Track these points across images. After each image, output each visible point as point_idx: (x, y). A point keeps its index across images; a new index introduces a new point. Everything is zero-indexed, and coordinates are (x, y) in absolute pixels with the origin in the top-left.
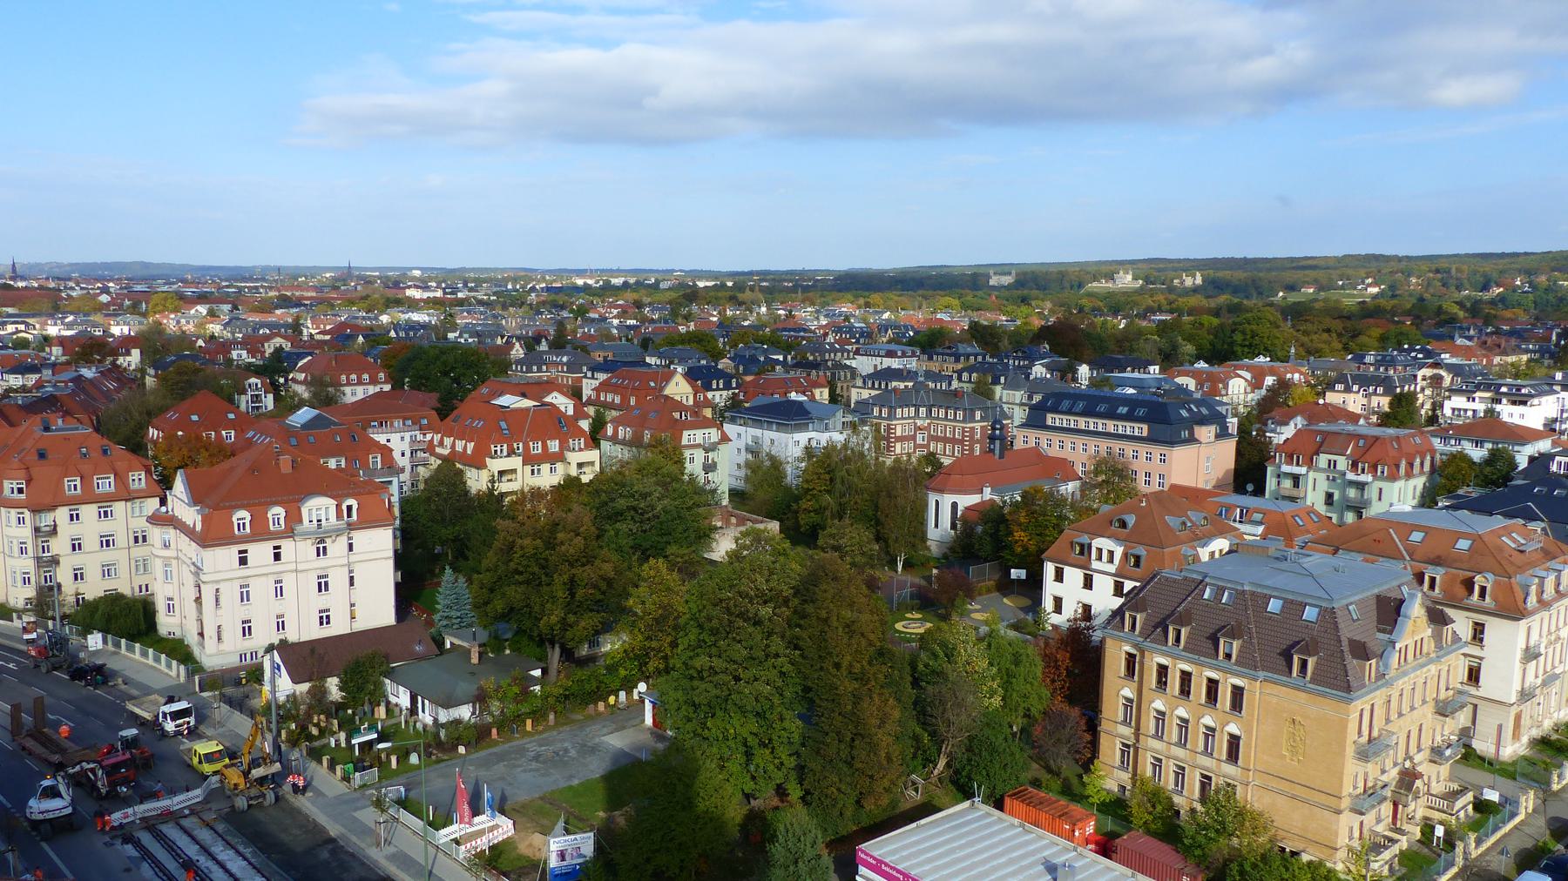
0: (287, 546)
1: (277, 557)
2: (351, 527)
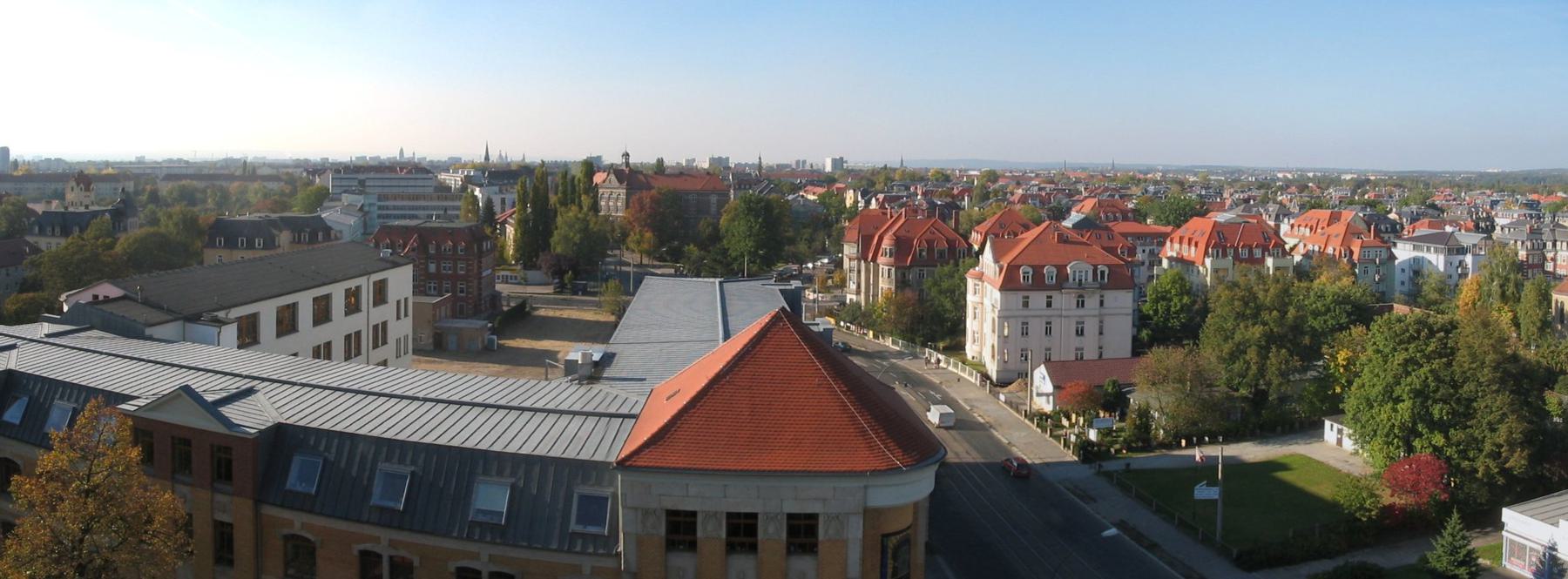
0: (1056, 295)
1: (1049, 305)
2: (1103, 287)
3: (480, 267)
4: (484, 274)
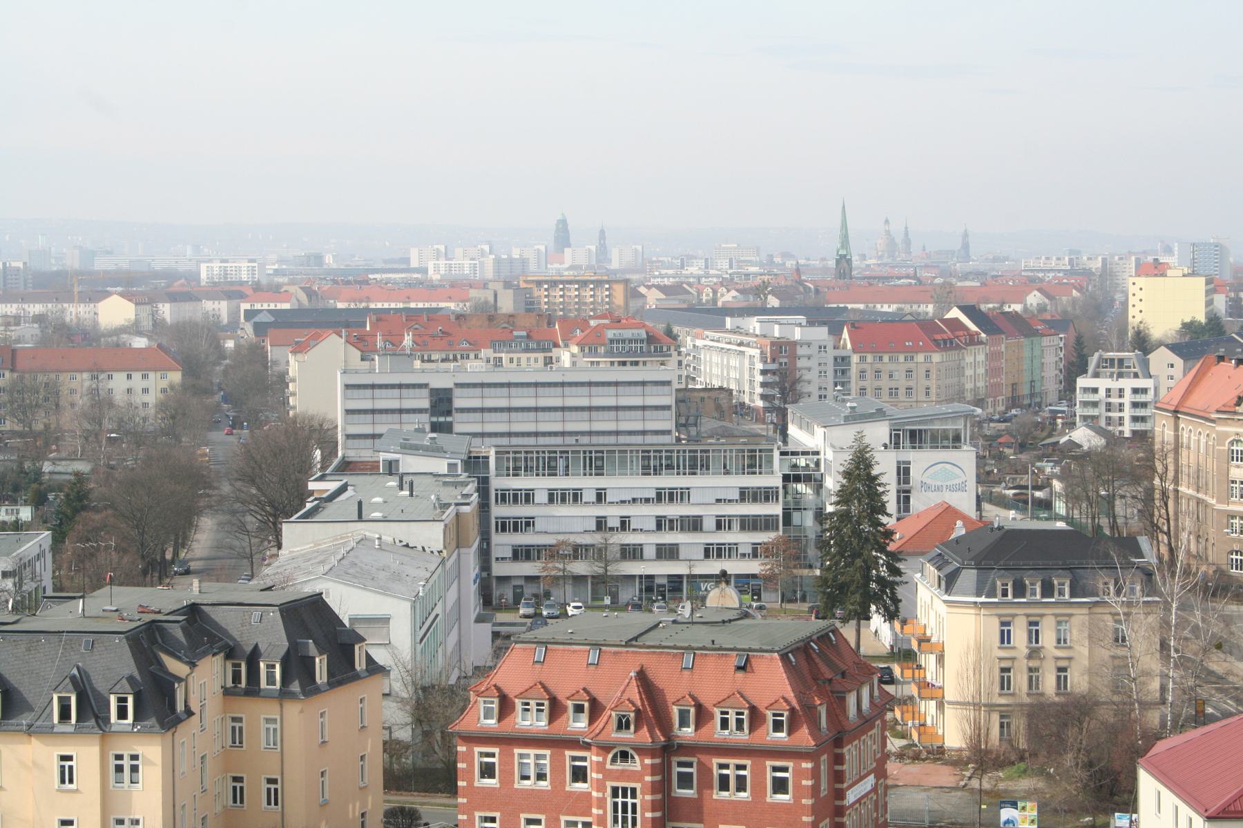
3: (838, 777)
4: (851, 796)
